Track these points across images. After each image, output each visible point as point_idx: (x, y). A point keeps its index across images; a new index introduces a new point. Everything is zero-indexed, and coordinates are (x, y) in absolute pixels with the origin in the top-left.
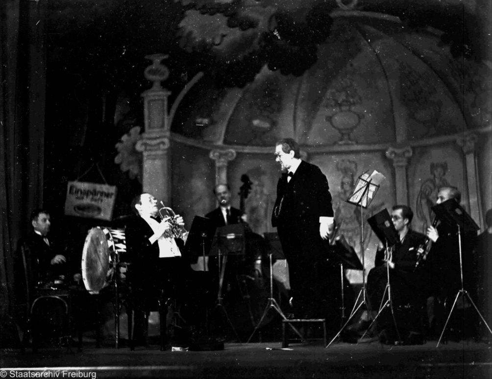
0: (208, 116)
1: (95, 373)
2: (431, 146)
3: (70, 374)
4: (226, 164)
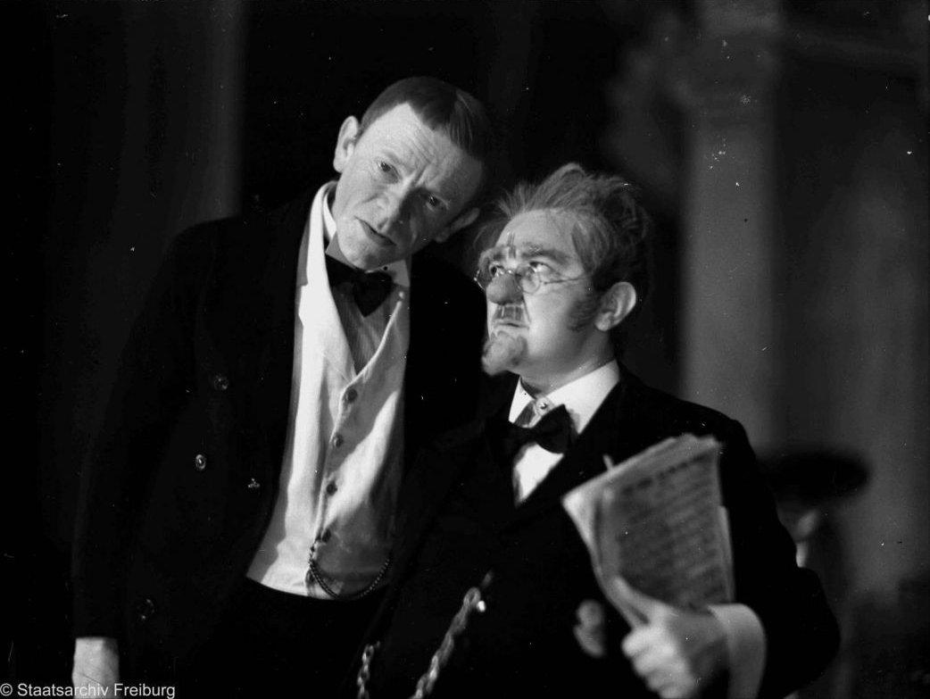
1: (173, 688)
3: (128, 690)
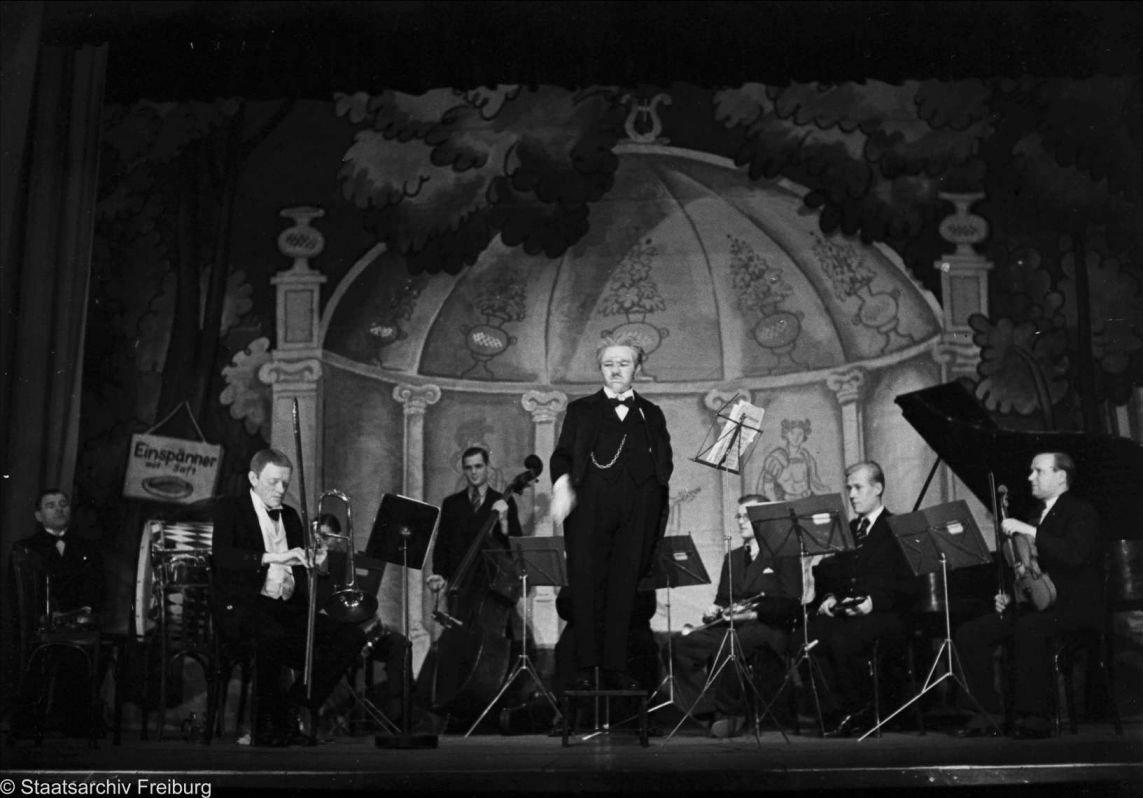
0: (393, 323)
2: (783, 389)
4: (422, 411)
